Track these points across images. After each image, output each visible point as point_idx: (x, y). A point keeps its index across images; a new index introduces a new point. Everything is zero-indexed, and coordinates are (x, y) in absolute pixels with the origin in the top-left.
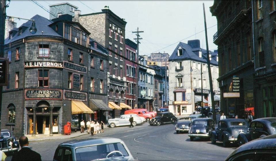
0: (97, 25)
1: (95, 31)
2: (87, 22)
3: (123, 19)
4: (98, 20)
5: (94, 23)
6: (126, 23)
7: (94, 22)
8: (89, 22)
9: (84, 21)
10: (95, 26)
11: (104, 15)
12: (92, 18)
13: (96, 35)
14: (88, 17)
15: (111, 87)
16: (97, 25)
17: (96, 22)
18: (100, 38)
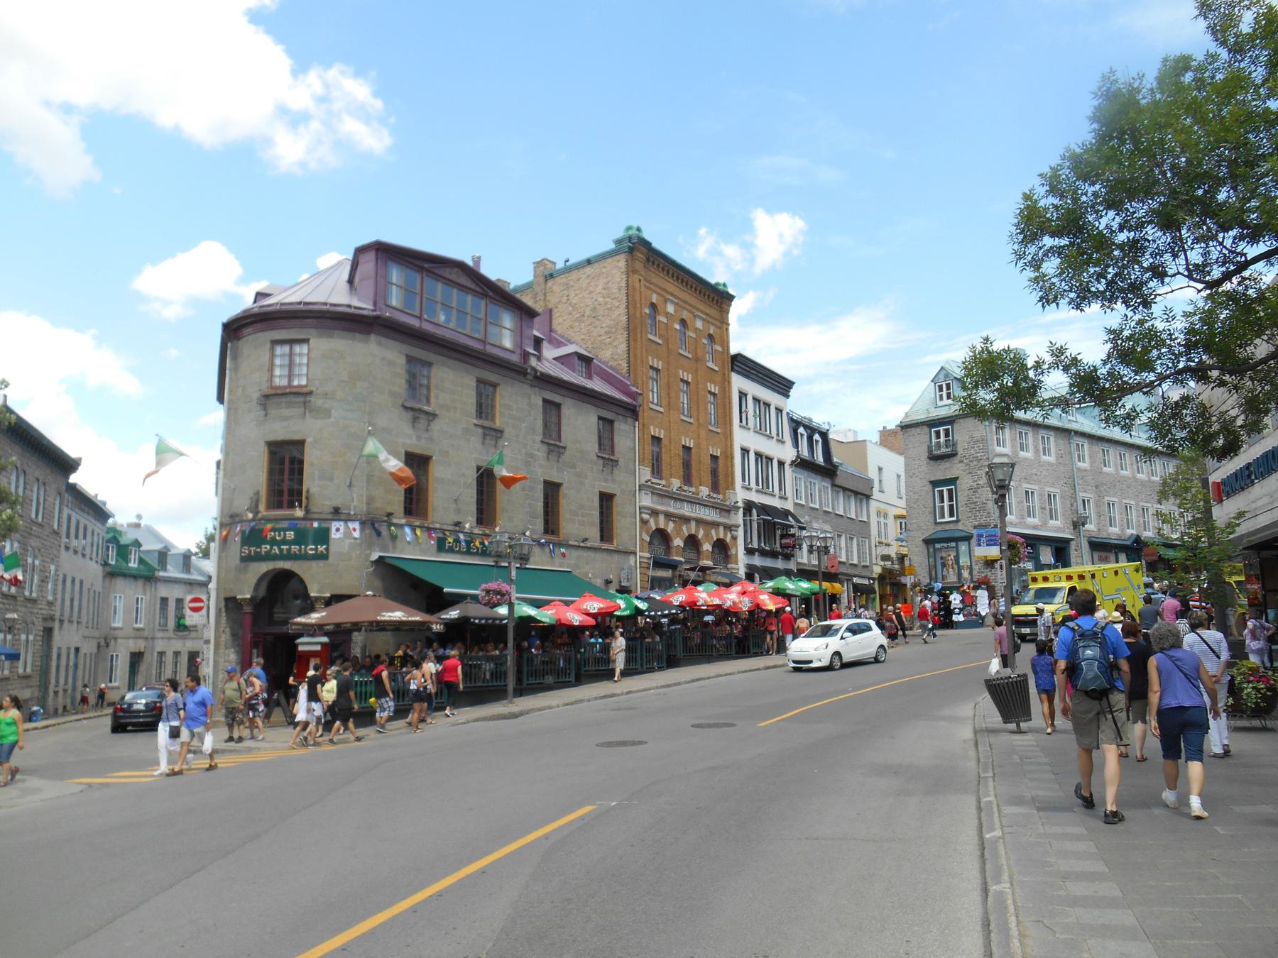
0: (601, 300)
1: (594, 320)
2: (572, 295)
3: (718, 284)
4: (605, 280)
5: (591, 292)
6: (730, 298)
7: (591, 289)
8: (576, 295)
9: (562, 291)
10: (596, 303)
11: (621, 262)
12: (584, 276)
13: (600, 336)
14: (574, 275)
15: (657, 522)
16: (601, 300)
17: (599, 288)
18: (610, 344)
